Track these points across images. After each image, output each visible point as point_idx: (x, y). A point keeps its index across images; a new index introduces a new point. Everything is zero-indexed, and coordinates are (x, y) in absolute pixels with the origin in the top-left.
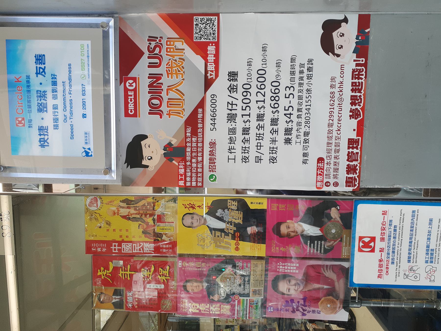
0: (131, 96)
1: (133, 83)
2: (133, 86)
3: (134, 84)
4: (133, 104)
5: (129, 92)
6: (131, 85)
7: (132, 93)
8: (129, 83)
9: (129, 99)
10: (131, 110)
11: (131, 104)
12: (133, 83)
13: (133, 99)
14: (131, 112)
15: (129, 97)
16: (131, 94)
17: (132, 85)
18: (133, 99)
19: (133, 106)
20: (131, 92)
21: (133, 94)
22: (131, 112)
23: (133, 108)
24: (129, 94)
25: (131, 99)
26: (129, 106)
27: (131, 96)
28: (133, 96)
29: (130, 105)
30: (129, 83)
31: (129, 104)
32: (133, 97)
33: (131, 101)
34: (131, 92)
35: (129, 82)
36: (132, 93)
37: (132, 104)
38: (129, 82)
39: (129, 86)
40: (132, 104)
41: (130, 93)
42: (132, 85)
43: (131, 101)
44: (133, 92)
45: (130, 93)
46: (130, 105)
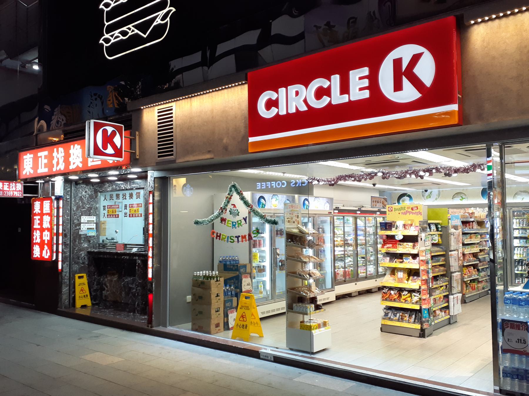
0: (345, 89)
2: (398, 87)
4: (303, 108)
17: (406, 83)
19: (293, 110)
23: (283, 112)
27: (345, 89)
28: (345, 99)
37: (305, 101)
40: (305, 101)
42: (406, 83)
44: (366, 94)
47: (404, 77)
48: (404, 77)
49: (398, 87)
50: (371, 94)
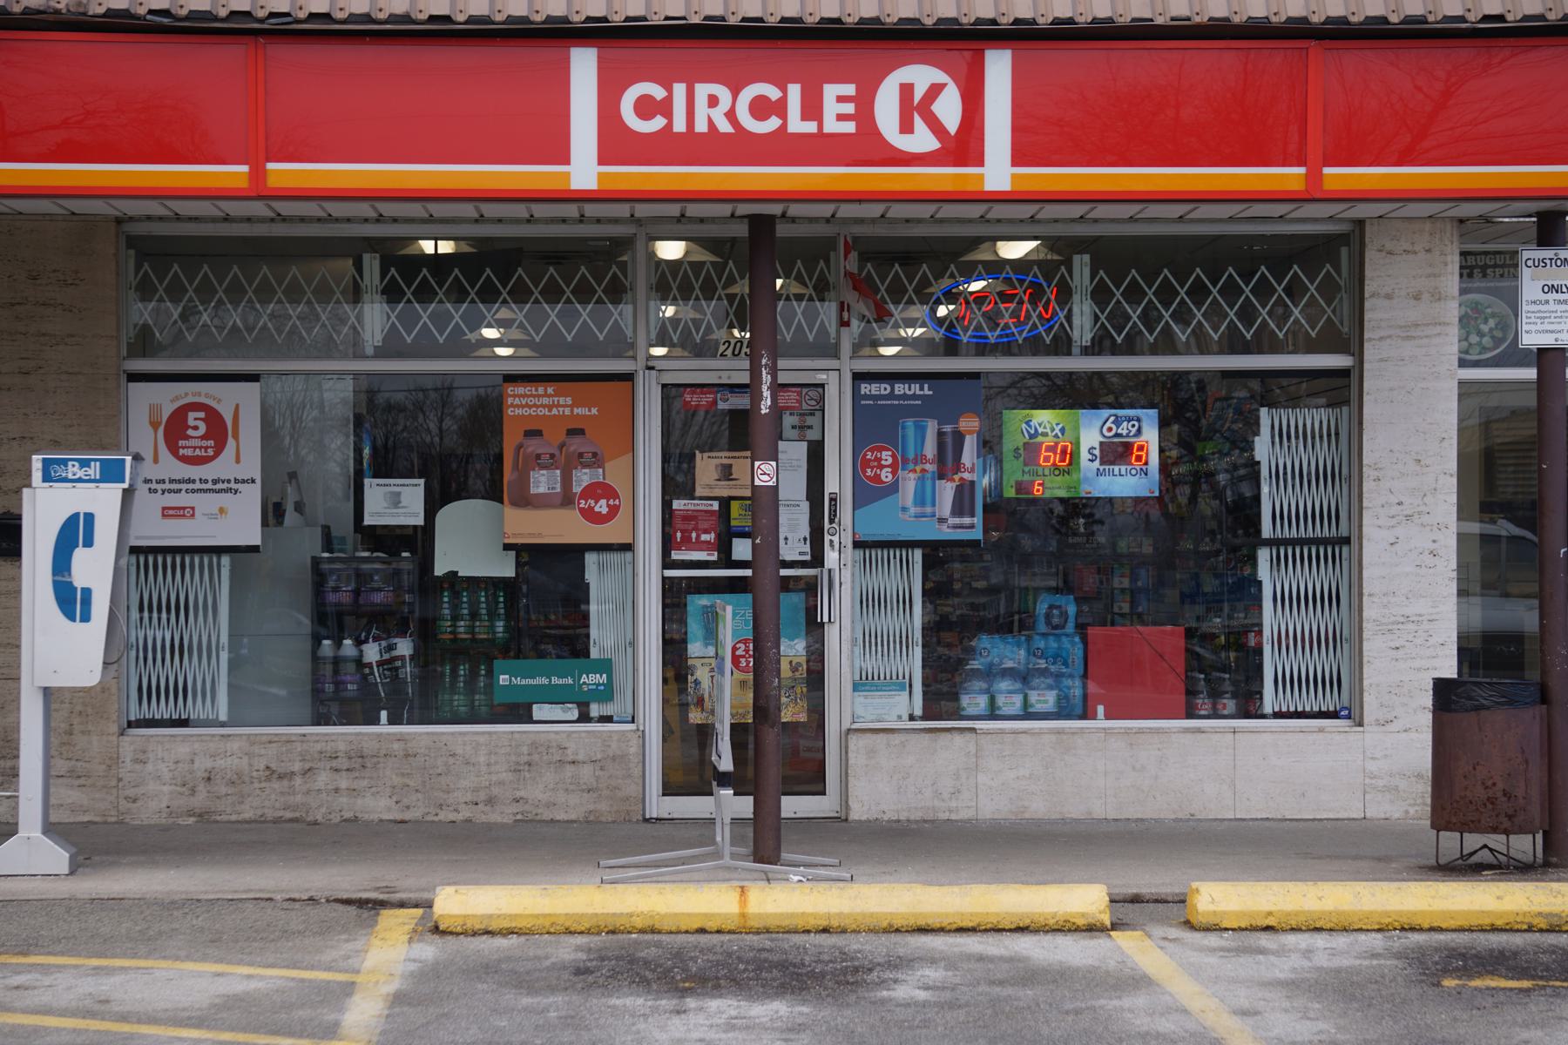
0: (812, 109)
2: (906, 127)
3: (922, 140)
4: (724, 127)
5: (849, 89)
6: (914, 108)
7: (841, 117)
8: (935, 90)
9: (773, 93)
10: (665, 107)
13: (773, 123)
14: (646, 108)
15: (794, 91)
16: (831, 108)
17: (919, 123)
18: (773, 123)
19: (701, 126)
20: (849, 108)
21: (832, 126)
22: (646, 108)
23: (680, 126)
24: (831, 91)
25: (780, 108)
26: (703, 90)
27: (812, 109)
28: (811, 127)
29: (713, 101)
30: (935, 90)
31: (723, 93)
32: (797, 125)
33: (761, 108)
34: (849, 108)
35: (945, 85)
36: (841, 117)
37: (731, 115)
38: (945, 85)
39: (906, 90)
40: (731, 115)
41: (841, 99)
42: (919, 123)
43: (761, 108)
44: (849, 127)
45: (841, 99)
46: (713, 101)
47: (916, 115)
48: (916, 115)
49: (906, 127)
50: (858, 127)
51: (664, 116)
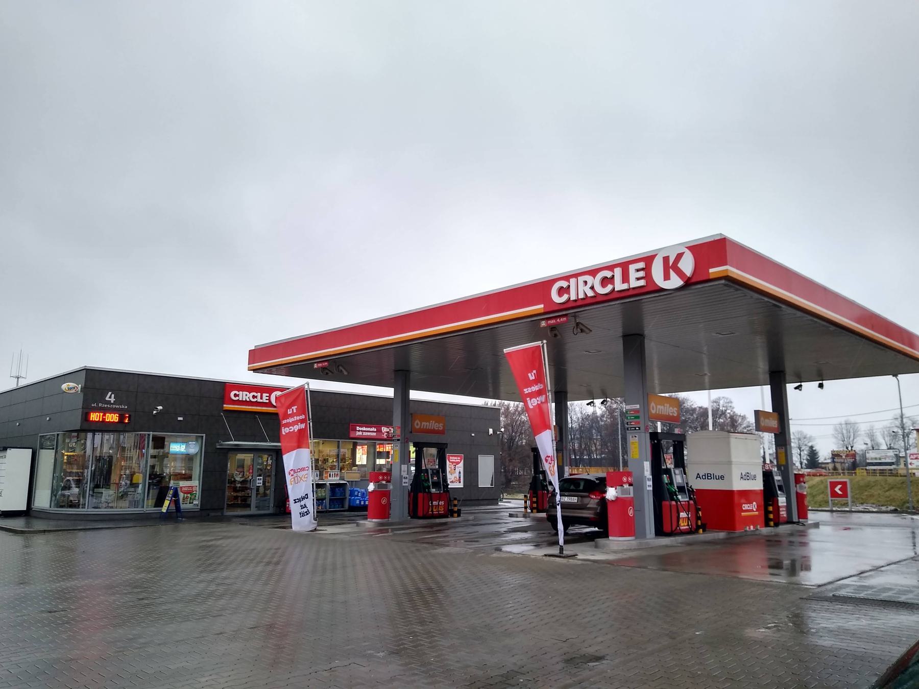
1: (680, 273)
2: (667, 277)
4: (590, 293)
8: (679, 256)
11: (589, 285)
12: (680, 273)
13: (609, 288)
14: (561, 291)
16: (633, 275)
17: (672, 274)
19: (581, 296)
20: (642, 274)
21: (634, 283)
22: (561, 291)
23: (573, 297)
27: (625, 278)
28: (625, 286)
29: (586, 283)
30: (679, 256)
32: (619, 286)
34: (642, 274)
36: (638, 279)
37: (592, 288)
39: (666, 259)
40: (592, 288)
42: (672, 274)
44: (642, 283)
45: (638, 270)
46: (586, 283)
47: (671, 270)
48: (671, 270)
49: (667, 277)
51: (567, 294)
